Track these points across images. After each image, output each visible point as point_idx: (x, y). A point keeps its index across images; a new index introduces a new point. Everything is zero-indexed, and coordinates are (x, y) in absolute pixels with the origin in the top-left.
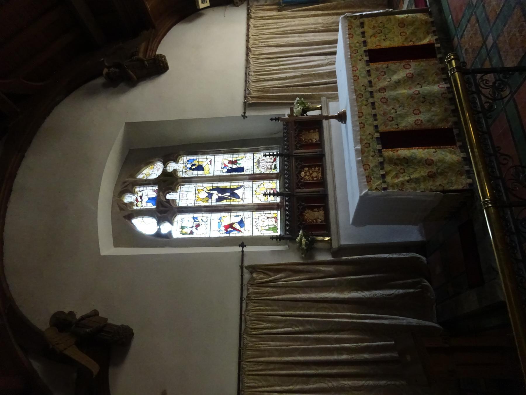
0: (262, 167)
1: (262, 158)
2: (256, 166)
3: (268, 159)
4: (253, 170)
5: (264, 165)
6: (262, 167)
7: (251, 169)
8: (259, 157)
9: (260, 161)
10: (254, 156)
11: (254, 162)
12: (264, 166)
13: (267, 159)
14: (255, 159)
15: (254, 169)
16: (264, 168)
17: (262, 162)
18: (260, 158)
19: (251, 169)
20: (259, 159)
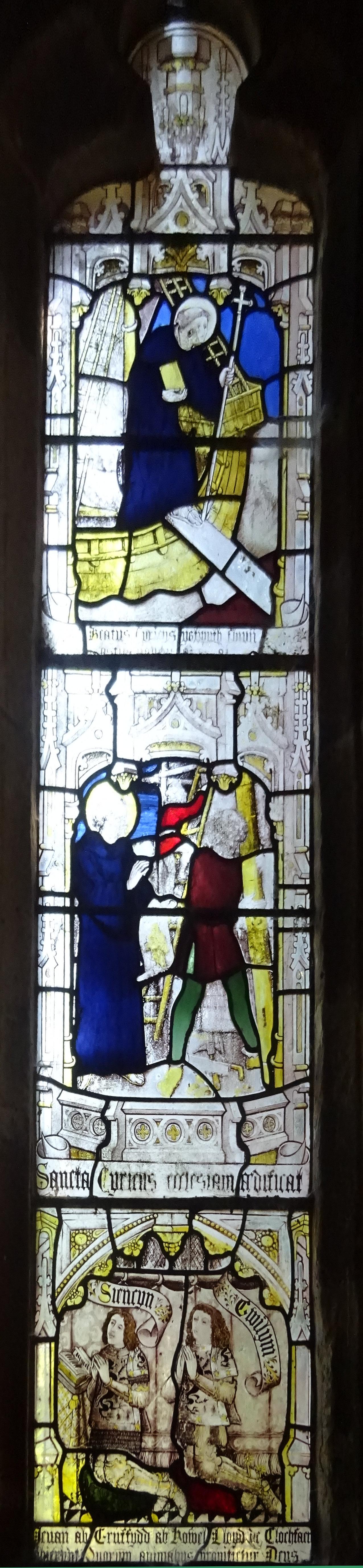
0: (130, 1323)
1: (253, 1320)
2: (149, 1236)
3: (230, 1405)
4: (92, 1203)
5: (147, 1342)
6: (130, 1323)
7: (115, 1167)
8: (257, 1282)
9: (205, 1296)
10: (275, 1220)
11: (194, 1206)
12: (132, 1343)
13: (226, 1391)
14: (231, 1221)
15: (109, 1204)
16: (107, 1350)
17: (186, 1324)
18: (253, 1294)
19: (115, 1167)
20: (240, 1283)
